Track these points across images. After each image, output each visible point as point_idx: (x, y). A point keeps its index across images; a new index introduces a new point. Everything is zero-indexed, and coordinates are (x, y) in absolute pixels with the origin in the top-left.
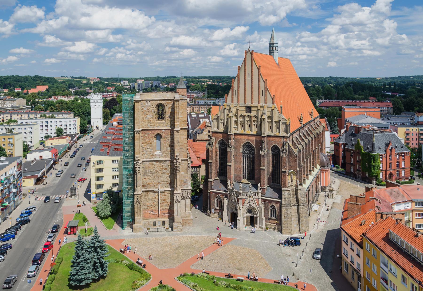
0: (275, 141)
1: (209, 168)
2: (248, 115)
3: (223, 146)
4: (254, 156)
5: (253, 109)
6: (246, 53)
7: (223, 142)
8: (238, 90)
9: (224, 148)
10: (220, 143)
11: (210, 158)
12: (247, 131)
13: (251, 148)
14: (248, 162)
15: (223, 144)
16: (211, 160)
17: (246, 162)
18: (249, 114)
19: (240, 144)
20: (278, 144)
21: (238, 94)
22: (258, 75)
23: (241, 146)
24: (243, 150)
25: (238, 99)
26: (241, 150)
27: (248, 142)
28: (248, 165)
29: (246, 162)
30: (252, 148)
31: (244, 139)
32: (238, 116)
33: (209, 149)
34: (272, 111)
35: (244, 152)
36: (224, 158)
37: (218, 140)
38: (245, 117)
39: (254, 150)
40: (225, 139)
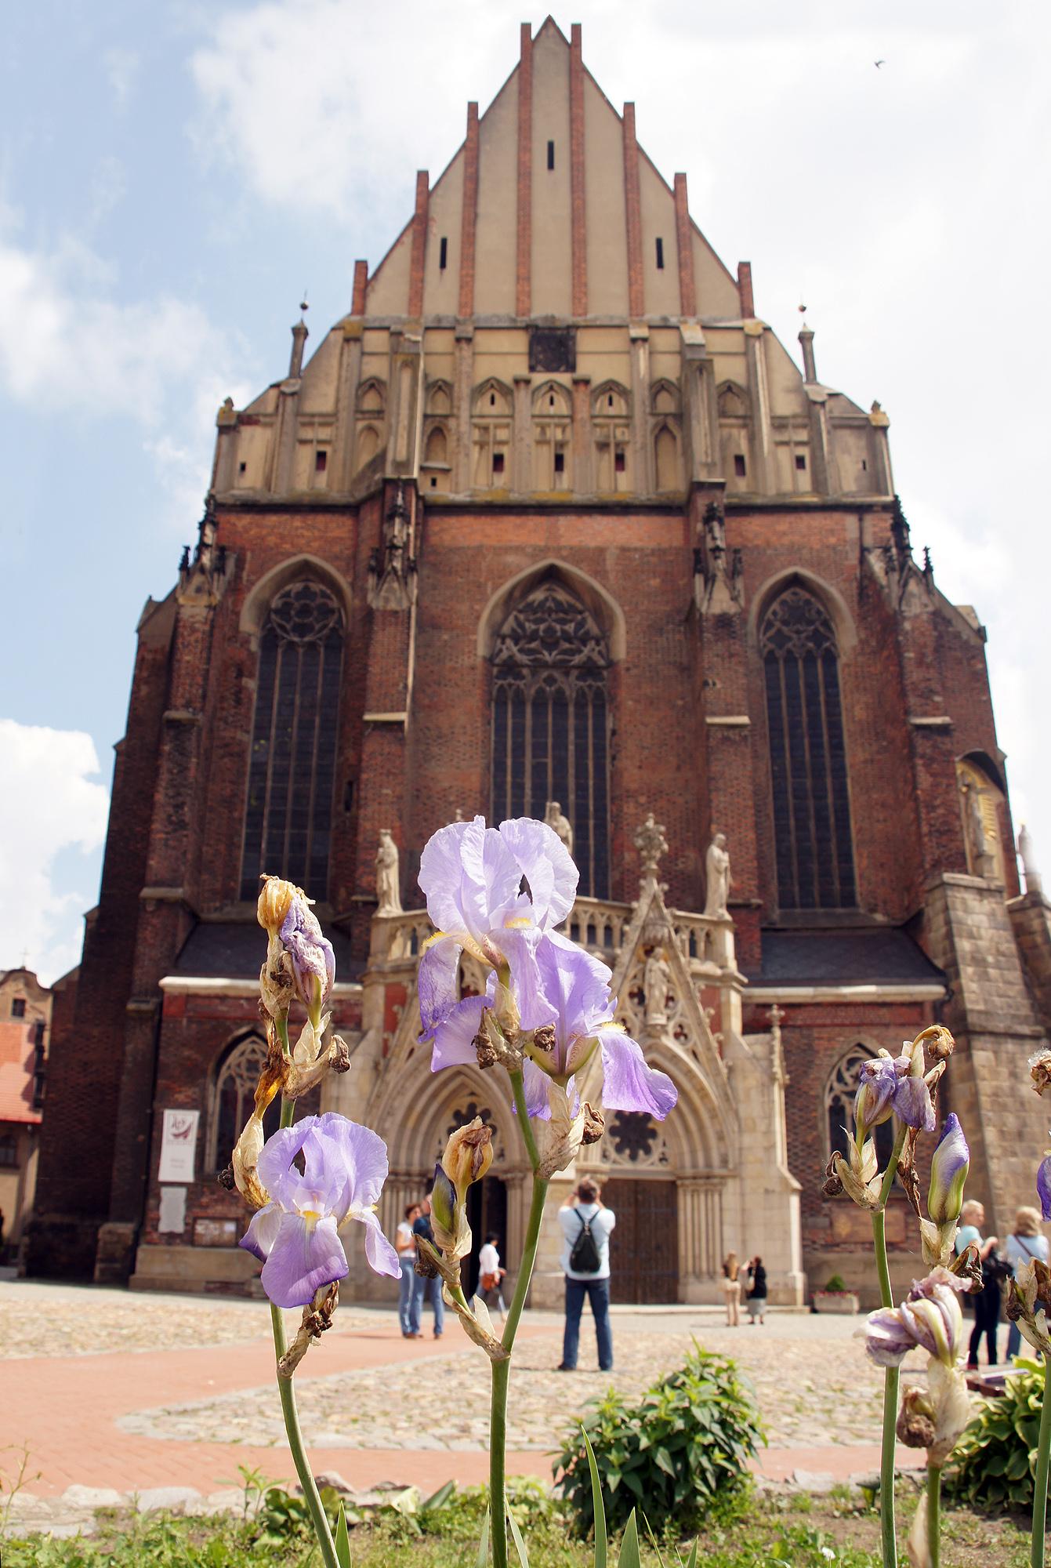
0: (794, 552)
1: (165, 777)
2: (551, 386)
3: (302, 630)
4: (598, 694)
5: (585, 342)
6: (528, 44)
7: (306, 593)
8: (469, 238)
9: (312, 646)
10: (275, 603)
11: (181, 692)
12: (541, 484)
13: (570, 628)
14: (539, 749)
15: (305, 611)
16: (187, 705)
17: (519, 749)
18: (564, 378)
19: (480, 586)
20: (817, 564)
21: (469, 259)
22: (625, 148)
23: (484, 599)
24: (496, 634)
25: (467, 283)
26: (481, 643)
27: (551, 575)
28: (539, 770)
29: (519, 749)
30: (581, 625)
31: (518, 549)
32: (463, 390)
33: (186, 613)
34: (747, 353)
35: (511, 657)
36: (306, 726)
37: (260, 572)
38: (522, 396)
39: (604, 637)
40: (334, 559)
